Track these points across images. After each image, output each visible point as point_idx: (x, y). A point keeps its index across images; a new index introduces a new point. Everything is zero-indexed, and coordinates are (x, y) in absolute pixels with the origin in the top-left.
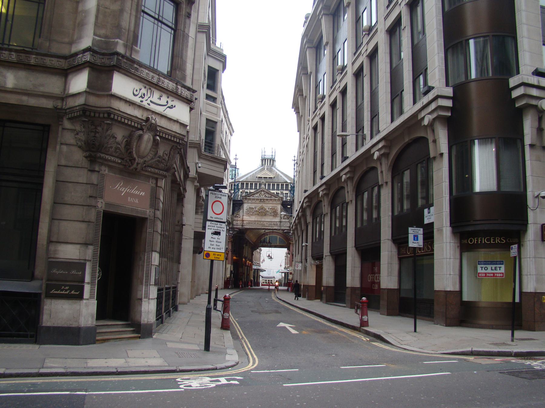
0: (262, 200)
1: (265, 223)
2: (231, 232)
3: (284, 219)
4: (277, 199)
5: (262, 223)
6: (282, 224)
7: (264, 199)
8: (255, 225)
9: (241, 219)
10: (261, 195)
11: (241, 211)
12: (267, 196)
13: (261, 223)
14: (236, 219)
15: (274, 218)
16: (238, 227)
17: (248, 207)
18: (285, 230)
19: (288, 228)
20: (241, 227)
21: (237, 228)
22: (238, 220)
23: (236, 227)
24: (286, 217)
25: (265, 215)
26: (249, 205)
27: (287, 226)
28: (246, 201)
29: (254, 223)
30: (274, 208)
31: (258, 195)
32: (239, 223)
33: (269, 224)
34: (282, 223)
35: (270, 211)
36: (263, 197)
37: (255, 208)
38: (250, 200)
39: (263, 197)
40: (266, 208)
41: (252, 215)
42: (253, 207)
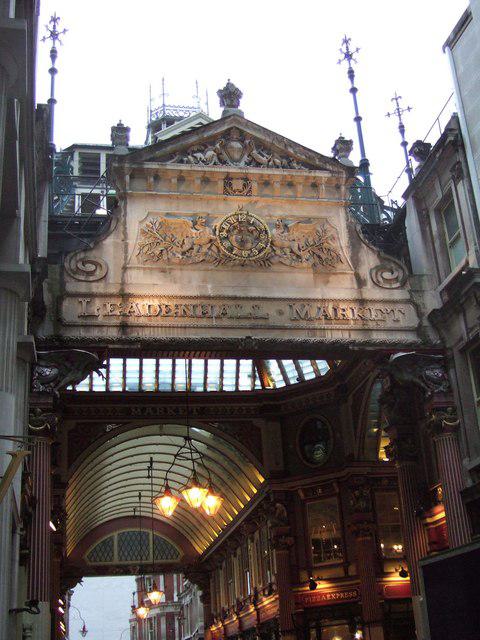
0: (237, 185)
1: (269, 310)
5: (247, 309)
11: (109, 242)
14: (82, 288)
18: (395, 347)
19: (411, 338)
22: (92, 296)
23: (82, 333)
25: (265, 263)
26: (162, 207)
27: (403, 324)
29: (199, 312)
31: (210, 153)
39: (242, 164)
40: (264, 223)
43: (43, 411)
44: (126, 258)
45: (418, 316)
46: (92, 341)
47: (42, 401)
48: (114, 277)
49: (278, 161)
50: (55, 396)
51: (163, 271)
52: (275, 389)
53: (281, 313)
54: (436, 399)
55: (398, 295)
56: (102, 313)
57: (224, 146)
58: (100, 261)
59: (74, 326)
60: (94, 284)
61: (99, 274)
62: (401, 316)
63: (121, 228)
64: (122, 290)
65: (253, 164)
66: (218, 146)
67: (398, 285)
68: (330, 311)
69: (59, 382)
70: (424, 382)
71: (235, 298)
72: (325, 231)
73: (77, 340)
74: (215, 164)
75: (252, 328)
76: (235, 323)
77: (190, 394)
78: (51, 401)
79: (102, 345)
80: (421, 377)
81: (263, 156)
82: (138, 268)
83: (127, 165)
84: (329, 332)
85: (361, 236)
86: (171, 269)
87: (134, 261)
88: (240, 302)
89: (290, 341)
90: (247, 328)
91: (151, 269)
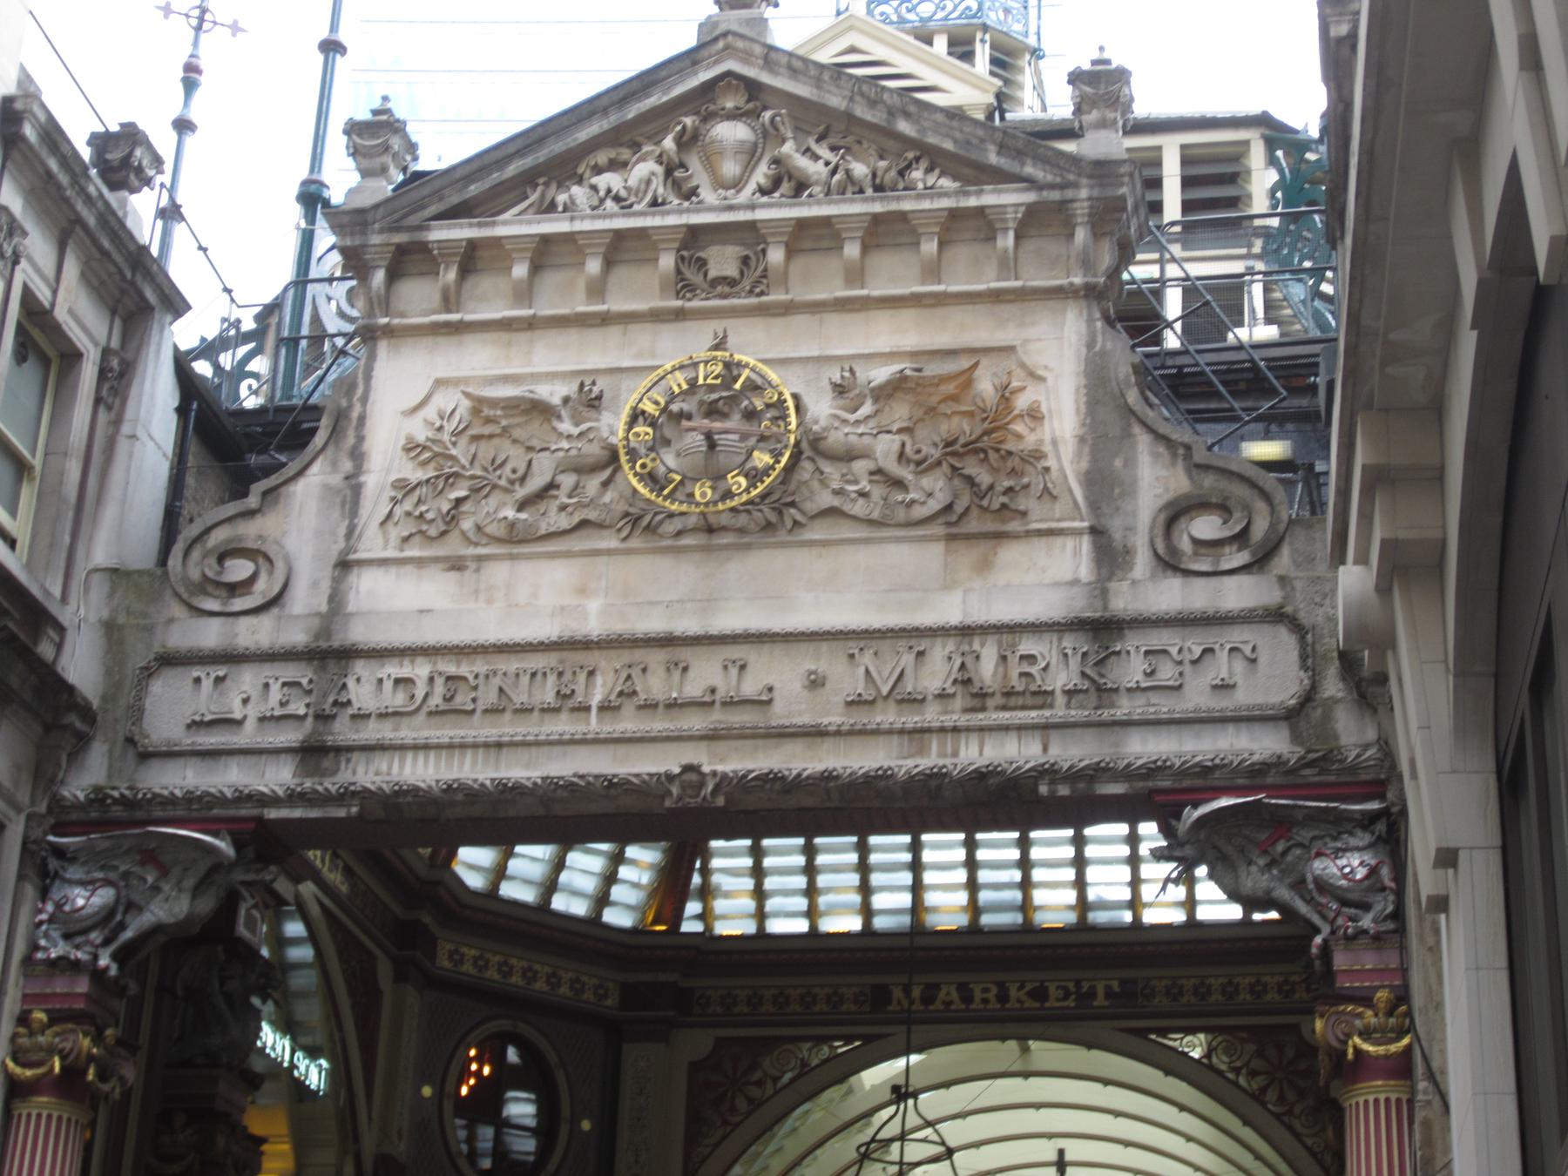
0: (723, 260)
3: (1170, 563)
4: (1010, 198)
5: (705, 674)
6: (1131, 670)
7: (750, 234)
8: (563, 725)
9: (298, 637)
10: (697, 173)
12: (816, 170)
13: (694, 688)
14: (209, 635)
15: (967, 556)
16: (230, 778)
17: (446, 400)
19: (1267, 744)
20: (279, 777)
21: (198, 808)
22: (232, 658)
24: (1206, 526)
27: (1243, 697)
30: (966, 380)
31: (645, 168)
33: (846, 679)
34: (1134, 643)
35: (885, 448)
38: (484, 284)
40: (785, 383)
41: (516, 538)
42: (553, 393)
43: (55, 1018)
44: (349, 535)
45: (1304, 666)
46: (220, 800)
47: (60, 986)
48: (306, 599)
49: (860, 169)
50: (98, 975)
51: (456, 565)
52: (708, 937)
53: (815, 683)
54: (1340, 961)
55: (1238, 594)
56: (253, 712)
57: (688, 141)
58: (272, 550)
59: (172, 754)
60: (245, 623)
61: (264, 587)
62: (1239, 666)
63: (351, 439)
64: (325, 631)
65: (786, 187)
66: (669, 143)
67: (1242, 558)
68: (987, 669)
69: (122, 926)
70: (1309, 901)
72: (1006, 395)
73: (171, 801)
74: (654, 203)
75: (711, 737)
77: (920, 941)
78: (82, 986)
79: (243, 812)
80: (1299, 885)
81: (816, 158)
82: (383, 562)
83: (376, 239)
84: (974, 741)
85: (1133, 397)
86: (480, 559)
87: (372, 544)
88: (684, 654)
89: (827, 777)
90: (691, 738)
91: (419, 562)
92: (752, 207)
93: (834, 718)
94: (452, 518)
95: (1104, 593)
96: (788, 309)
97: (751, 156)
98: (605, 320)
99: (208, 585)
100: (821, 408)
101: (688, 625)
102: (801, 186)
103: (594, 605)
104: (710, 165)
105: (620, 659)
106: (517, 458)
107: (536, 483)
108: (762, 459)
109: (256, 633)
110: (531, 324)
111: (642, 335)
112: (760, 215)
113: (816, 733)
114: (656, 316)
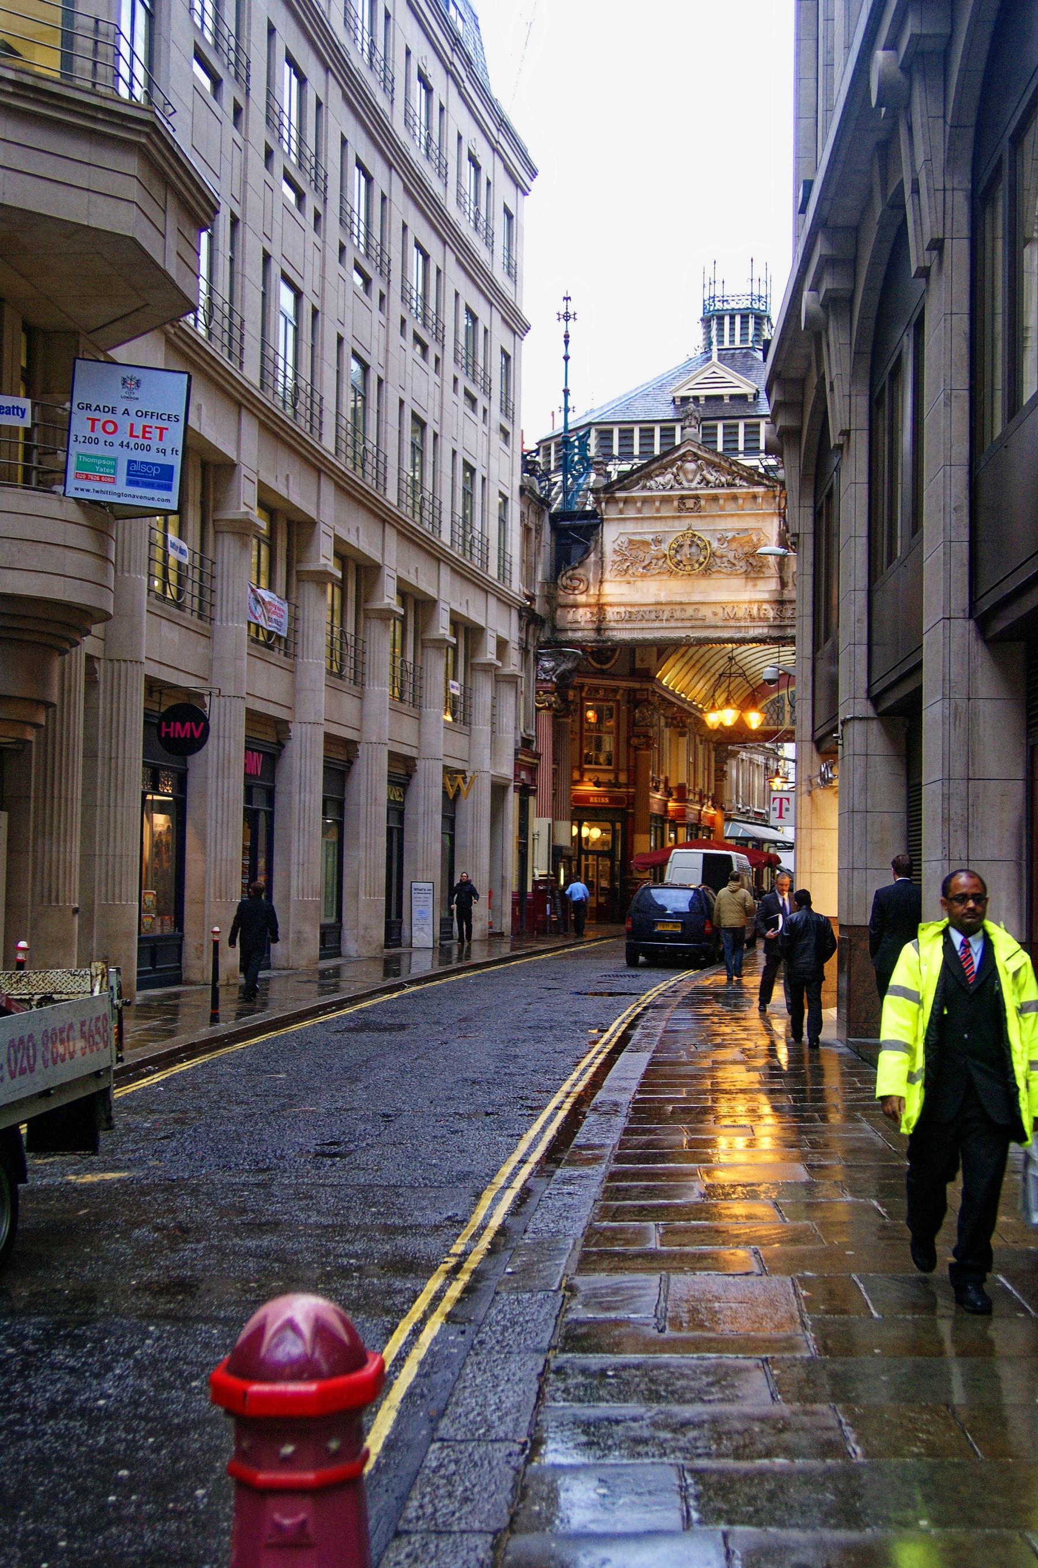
0: (690, 503)
1: (706, 612)
2: (548, 665)
5: (690, 611)
6: (789, 614)
7: (697, 497)
8: (657, 624)
10: (681, 477)
12: (711, 478)
13: (687, 615)
15: (750, 584)
16: (579, 635)
17: (623, 539)
25: (707, 571)
26: (630, 527)
28: (611, 512)
31: (669, 477)
32: (583, 616)
34: (788, 606)
36: (692, 485)
37: (658, 542)
39: (694, 485)
40: (706, 537)
41: (643, 576)
42: (649, 538)
49: (723, 479)
71: (681, 603)
75: (692, 627)
76: (680, 625)
92: (696, 489)
93: (720, 624)
94: (626, 571)
95: (782, 594)
96: (705, 517)
97: (695, 473)
98: (660, 518)
99: (566, 588)
100: (715, 545)
101: (685, 599)
102: (708, 482)
103: (663, 594)
104: (685, 474)
105: (669, 608)
106: (641, 555)
107: (646, 562)
108: (702, 559)
109: (582, 599)
110: (642, 518)
111: (670, 522)
112: (699, 492)
113: (716, 627)
114: (674, 517)
